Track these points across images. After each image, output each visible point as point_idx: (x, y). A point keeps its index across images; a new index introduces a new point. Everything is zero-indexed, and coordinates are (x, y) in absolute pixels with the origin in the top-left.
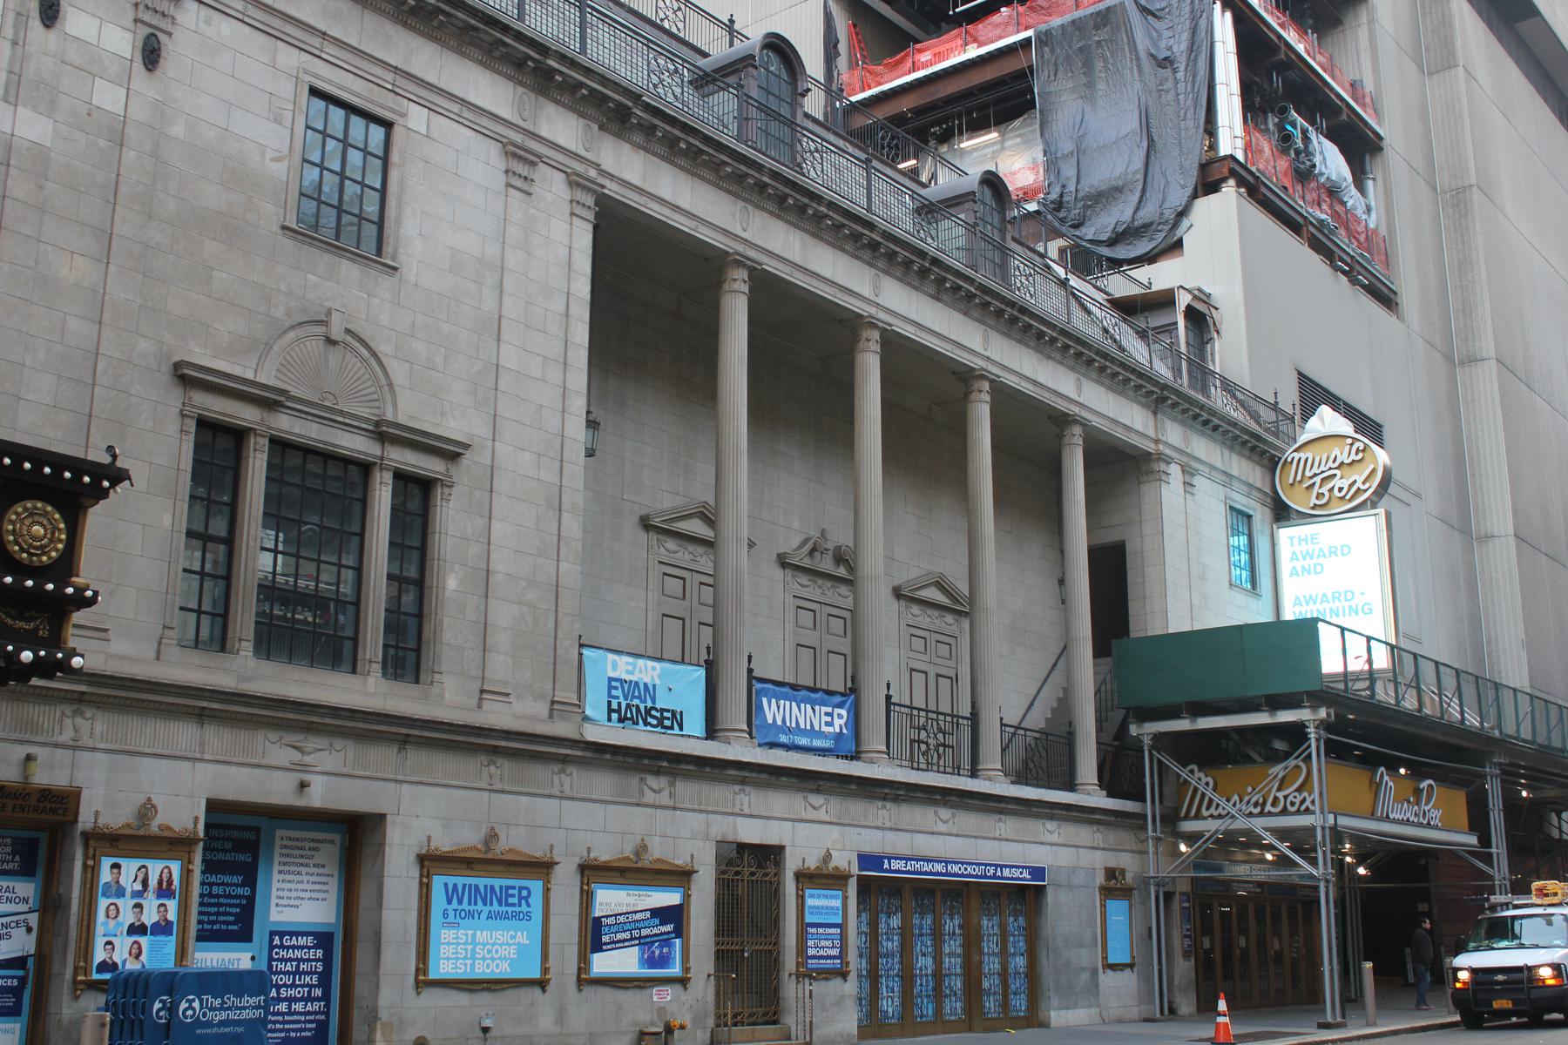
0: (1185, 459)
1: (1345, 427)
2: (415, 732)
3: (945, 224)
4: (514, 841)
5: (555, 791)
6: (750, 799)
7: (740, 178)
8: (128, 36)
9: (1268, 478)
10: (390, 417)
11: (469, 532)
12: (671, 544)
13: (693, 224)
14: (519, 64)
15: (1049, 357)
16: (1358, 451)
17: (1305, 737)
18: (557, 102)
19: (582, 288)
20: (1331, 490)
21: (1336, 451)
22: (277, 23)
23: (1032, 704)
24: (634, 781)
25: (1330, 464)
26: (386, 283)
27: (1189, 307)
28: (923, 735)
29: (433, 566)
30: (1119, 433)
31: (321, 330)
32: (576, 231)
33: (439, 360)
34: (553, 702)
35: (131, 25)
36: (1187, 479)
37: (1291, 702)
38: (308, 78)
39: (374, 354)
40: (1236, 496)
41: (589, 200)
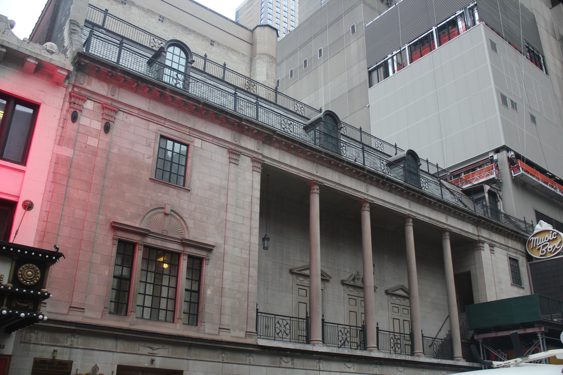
0: (490, 242)
1: (549, 227)
2: (194, 342)
3: (397, 168)
5: (247, 363)
7: (314, 156)
8: (100, 123)
9: (523, 247)
10: (187, 237)
11: (215, 275)
12: (301, 279)
13: (298, 172)
14: (233, 124)
15: (434, 209)
16: (554, 235)
17: (537, 338)
18: (247, 135)
19: (257, 194)
20: (546, 250)
21: (547, 236)
22: (149, 116)
23: (440, 330)
24: (278, 359)
25: (545, 240)
26: (187, 194)
27: (489, 190)
28: (399, 341)
29: (202, 286)
30: (463, 234)
31: (163, 210)
32: (254, 175)
33: (205, 219)
34: (247, 332)
35: (101, 120)
36: (491, 248)
37: (531, 325)
38: (160, 132)
39: (181, 218)
40: (511, 254)
41: (259, 166)
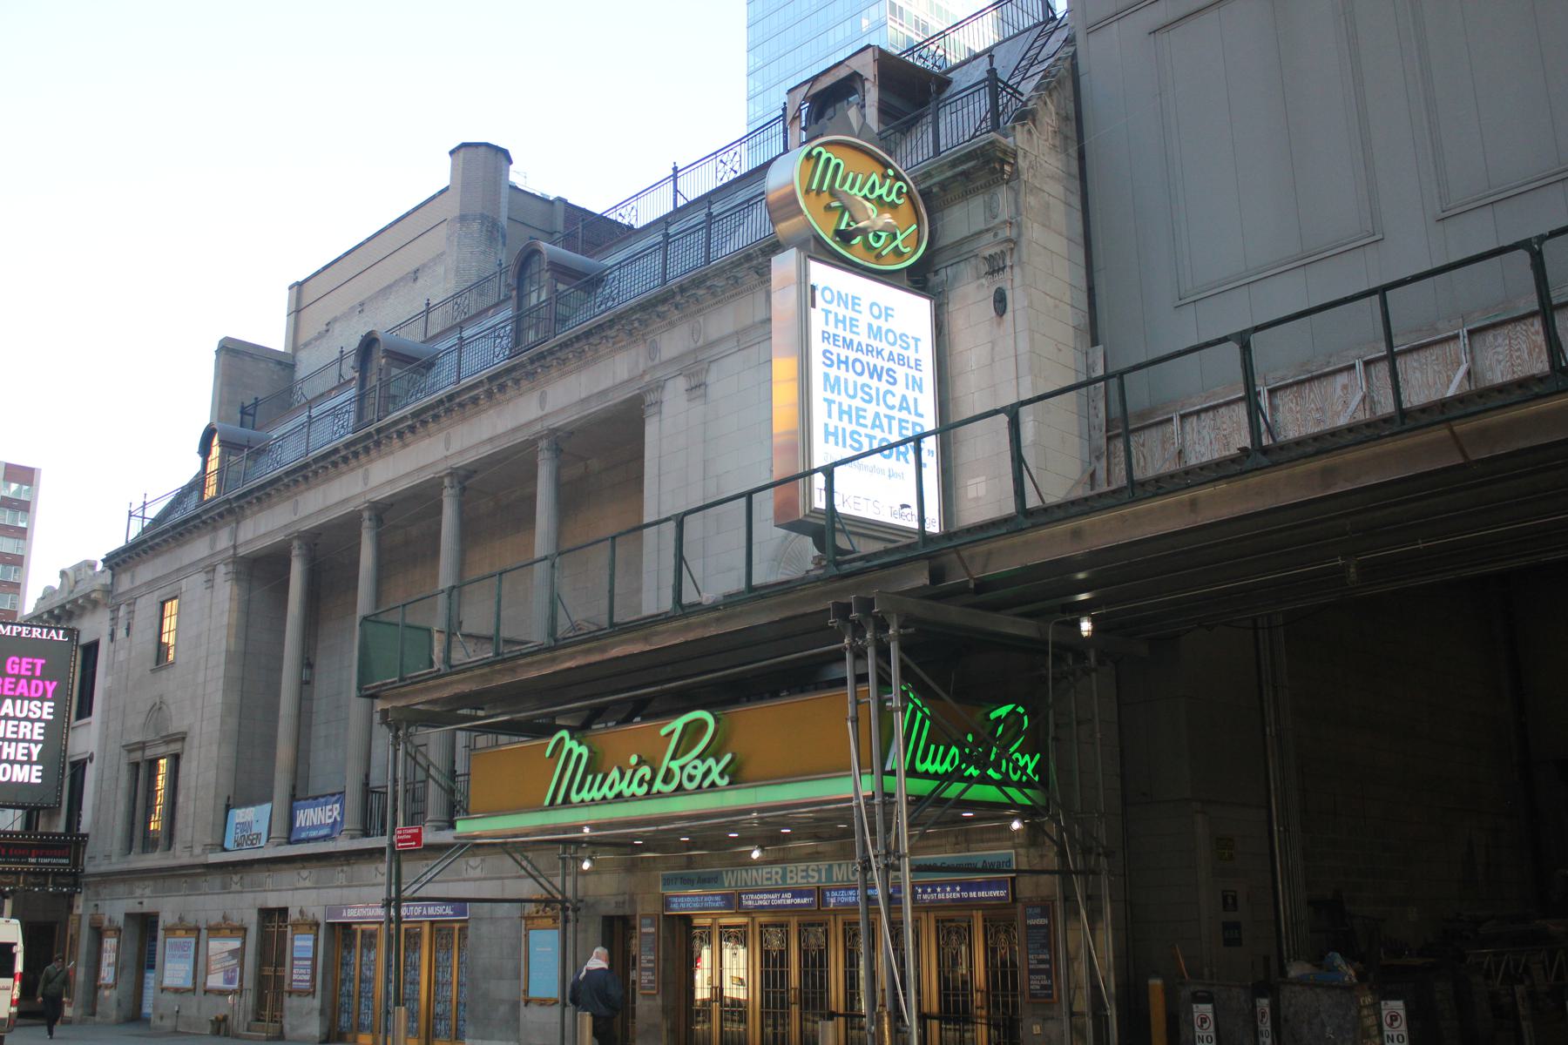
4: (191, 920)
6: (267, 878)
30: (594, 407)
41: (230, 568)
